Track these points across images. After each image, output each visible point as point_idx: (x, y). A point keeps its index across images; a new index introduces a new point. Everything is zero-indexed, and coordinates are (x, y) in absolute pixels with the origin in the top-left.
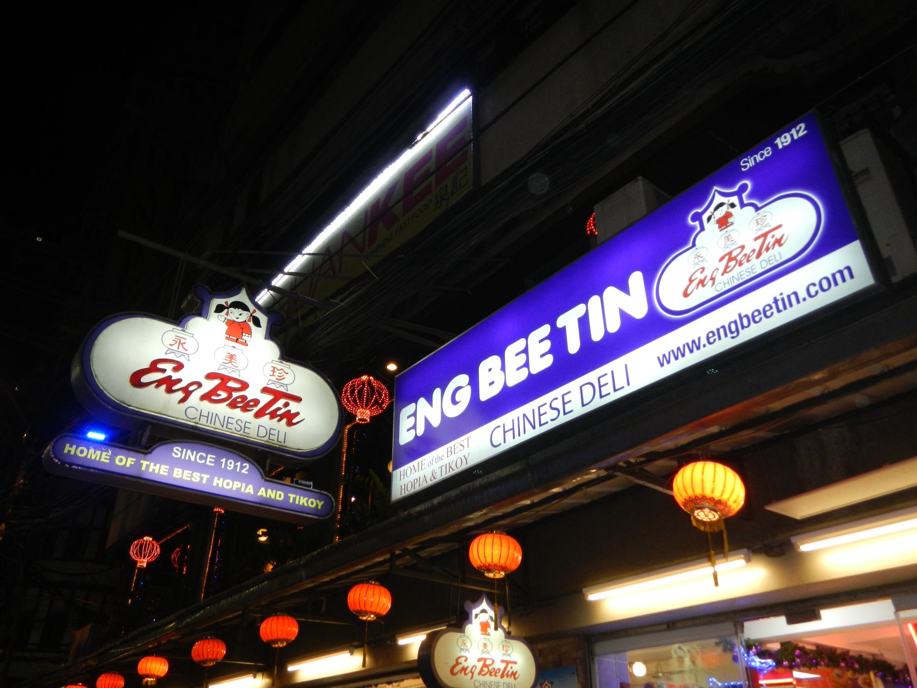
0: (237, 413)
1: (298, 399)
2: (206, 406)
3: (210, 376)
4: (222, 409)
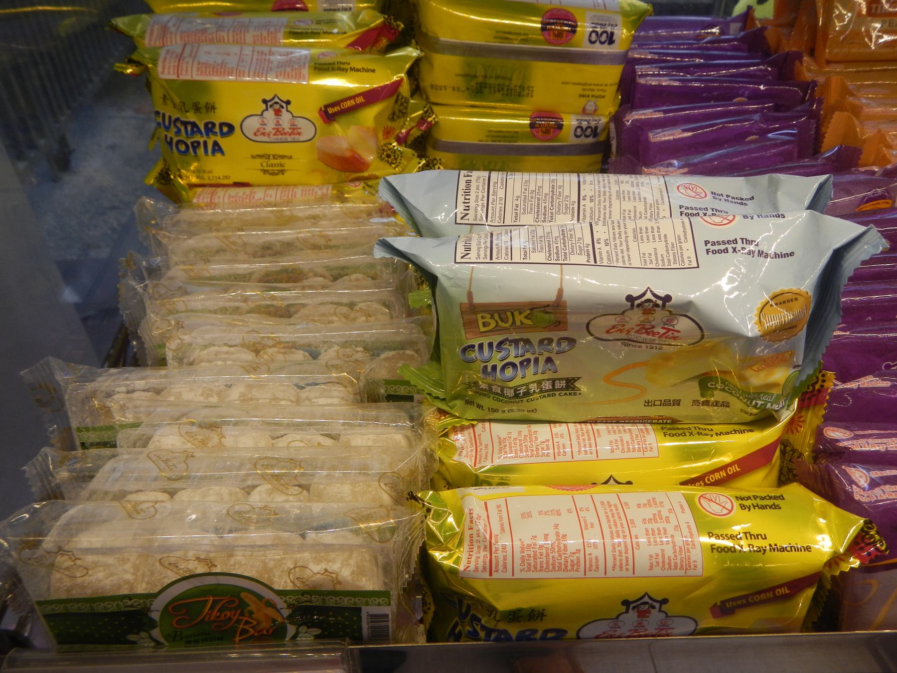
0: (284, 136)
1: (300, 128)
2: (275, 137)
3: (274, 129)
4: (280, 137)
